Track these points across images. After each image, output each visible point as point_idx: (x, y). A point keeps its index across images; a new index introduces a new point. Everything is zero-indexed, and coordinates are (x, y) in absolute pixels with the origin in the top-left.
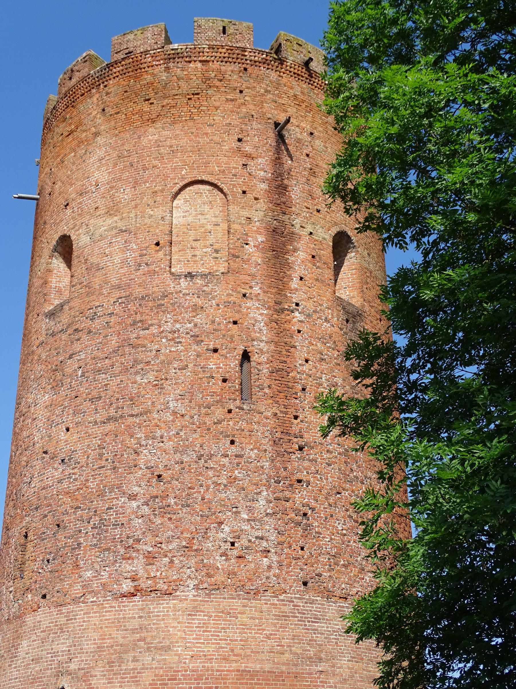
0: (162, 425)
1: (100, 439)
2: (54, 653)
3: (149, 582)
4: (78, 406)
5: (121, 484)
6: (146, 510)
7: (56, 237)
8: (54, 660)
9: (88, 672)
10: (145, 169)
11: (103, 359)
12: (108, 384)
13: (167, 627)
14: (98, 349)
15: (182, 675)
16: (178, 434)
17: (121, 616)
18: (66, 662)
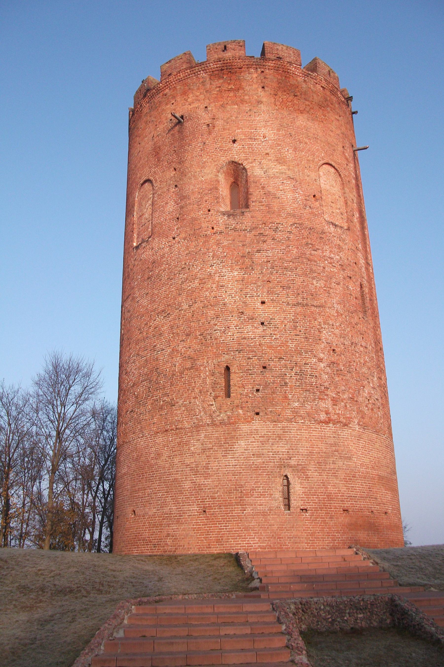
2: (275, 452)
3: (336, 416)
4: (271, 288)
5: (312, 349)
6: (329, 370)
7: (224, 160)
8: (276, 457)
9: (305, 467)
10: (300, 142)
11: (288, 261)
12: (295, 280)
13: (348, 445)
14: (283, 253)
15: (358, 475)
17: (323, 435)
18: (286, 459)
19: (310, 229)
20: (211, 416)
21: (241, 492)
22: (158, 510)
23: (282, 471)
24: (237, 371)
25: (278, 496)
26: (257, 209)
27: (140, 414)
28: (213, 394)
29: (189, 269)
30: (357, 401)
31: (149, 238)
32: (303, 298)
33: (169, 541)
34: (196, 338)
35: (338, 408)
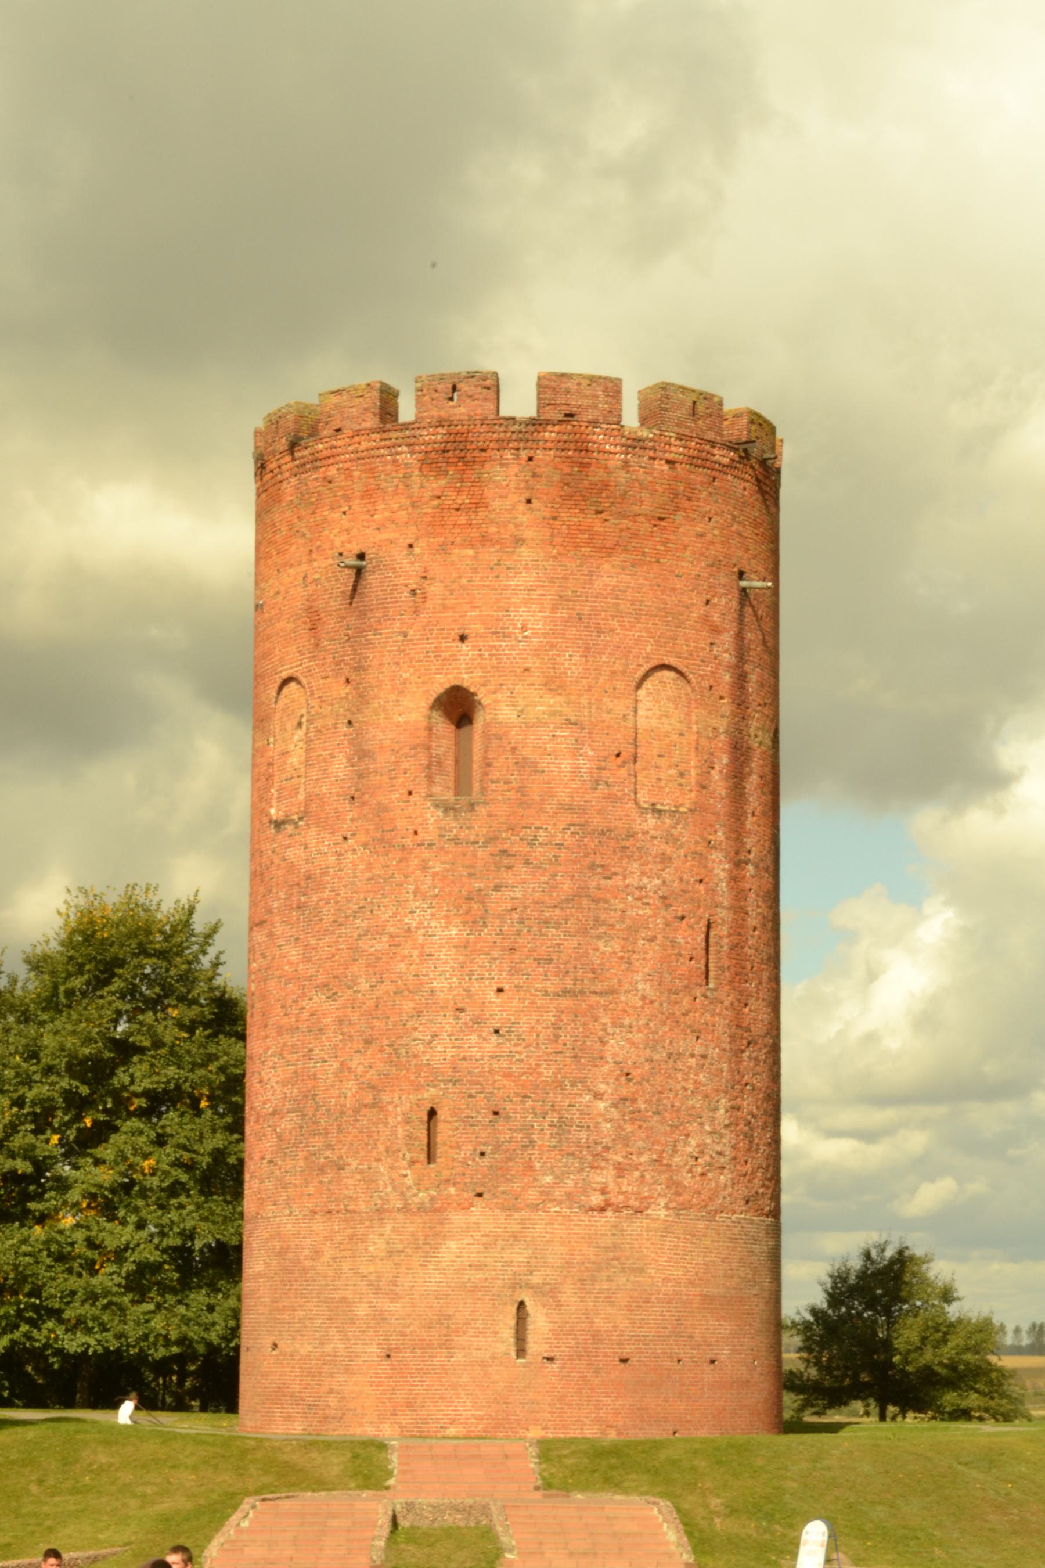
0: (630, 1011)
1: (554, 1016)
10: (600, 632)
16: (647, 1024)
18: (525, 1275)
19: (602, 833)
20: (402, 1194)
21: (448, 1327)
22: (315, 1348)
23: (516, 1294)
24: (450, 1119)
25: (508, 1335)
26: (500, 798)
27: (286, 1172)
28: (408, 1156)
29: (372, 911)
30: (669, 1165)
31: (301, 819)
32: (576, 980)
33: (333, 1401)
34: (381, 1051)
35: (625, 1182)
